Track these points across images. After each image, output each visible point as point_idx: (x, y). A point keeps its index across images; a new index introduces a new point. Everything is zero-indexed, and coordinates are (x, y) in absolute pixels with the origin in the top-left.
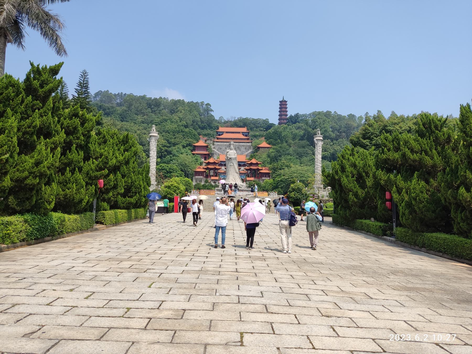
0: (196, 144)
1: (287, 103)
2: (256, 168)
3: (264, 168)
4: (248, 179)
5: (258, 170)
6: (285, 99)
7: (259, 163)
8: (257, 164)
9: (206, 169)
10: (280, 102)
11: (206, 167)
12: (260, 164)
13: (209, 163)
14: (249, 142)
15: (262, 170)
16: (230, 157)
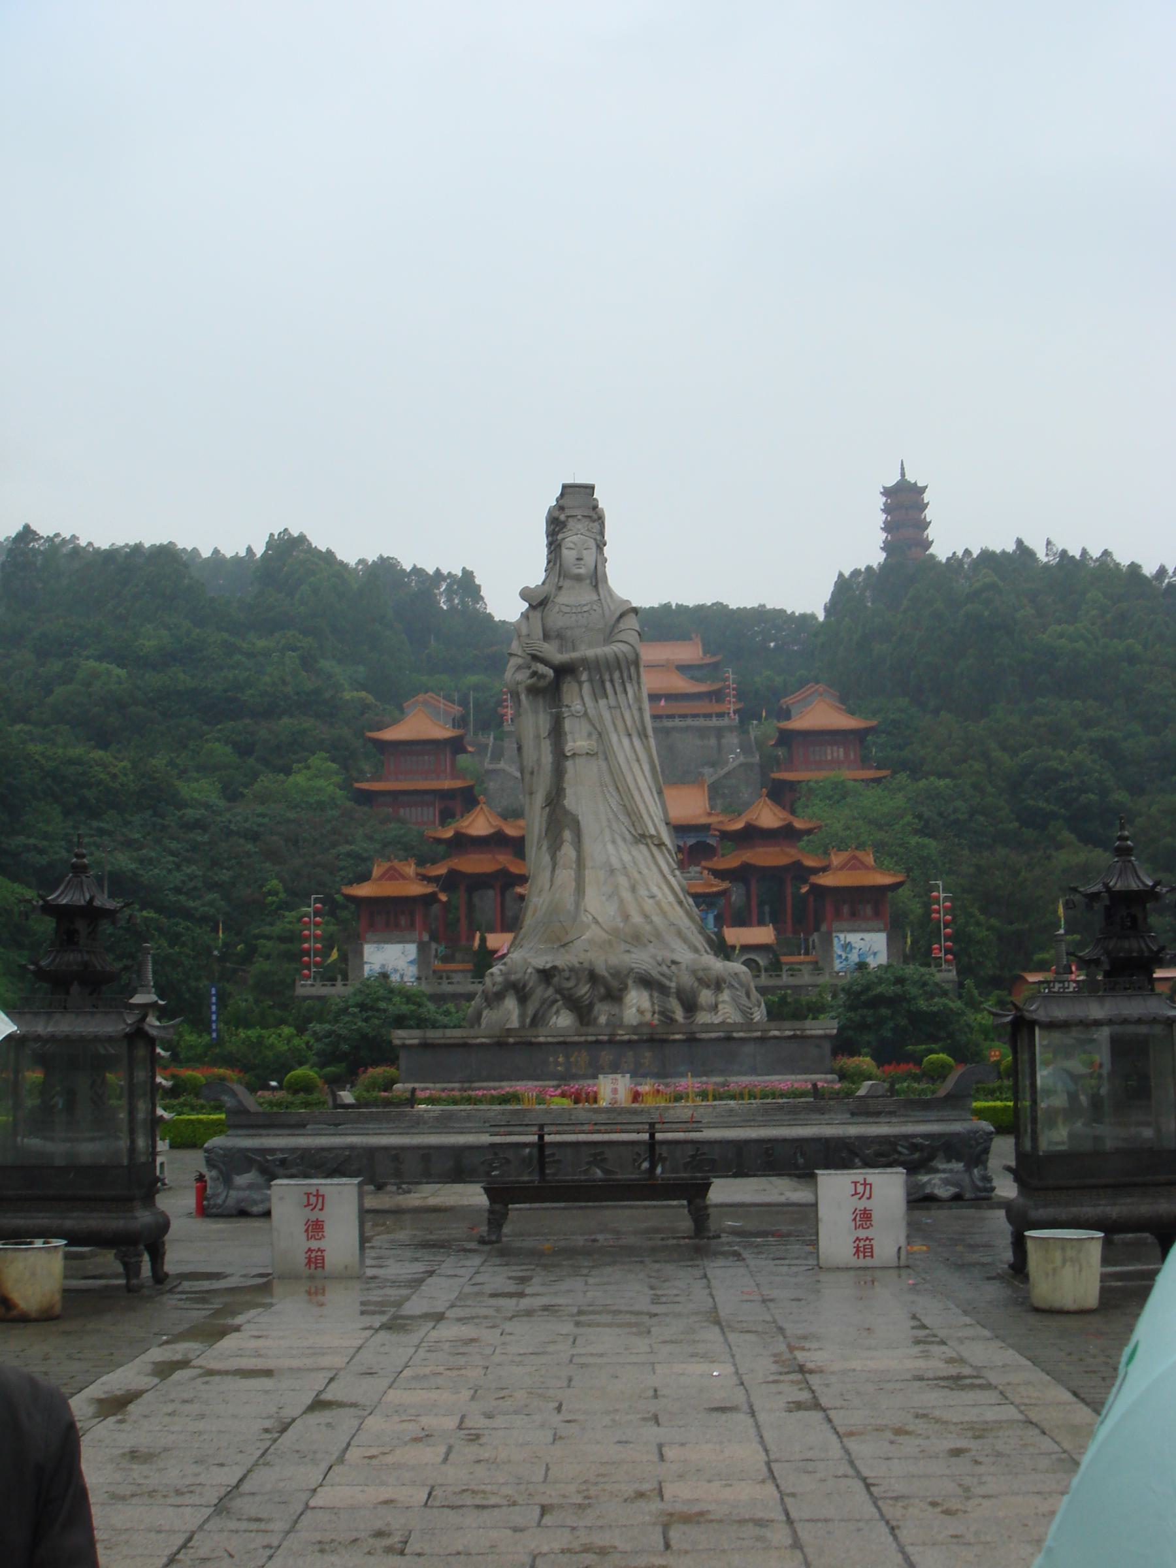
0: (389, 735)
1: (927, 497)
2: (783, 861)
3: (836, 860)
4: (735, 936)
5: (800, 872)
6: (911, 478)
7: (798, 824)
8: (787, 834)
9: (451, 881)
10: (887, 492)
11: (441, 870)
12: (809, 832)
13: (462, 843)
14: (721, 715)
15: (824, 869)
16: (561, 658)
